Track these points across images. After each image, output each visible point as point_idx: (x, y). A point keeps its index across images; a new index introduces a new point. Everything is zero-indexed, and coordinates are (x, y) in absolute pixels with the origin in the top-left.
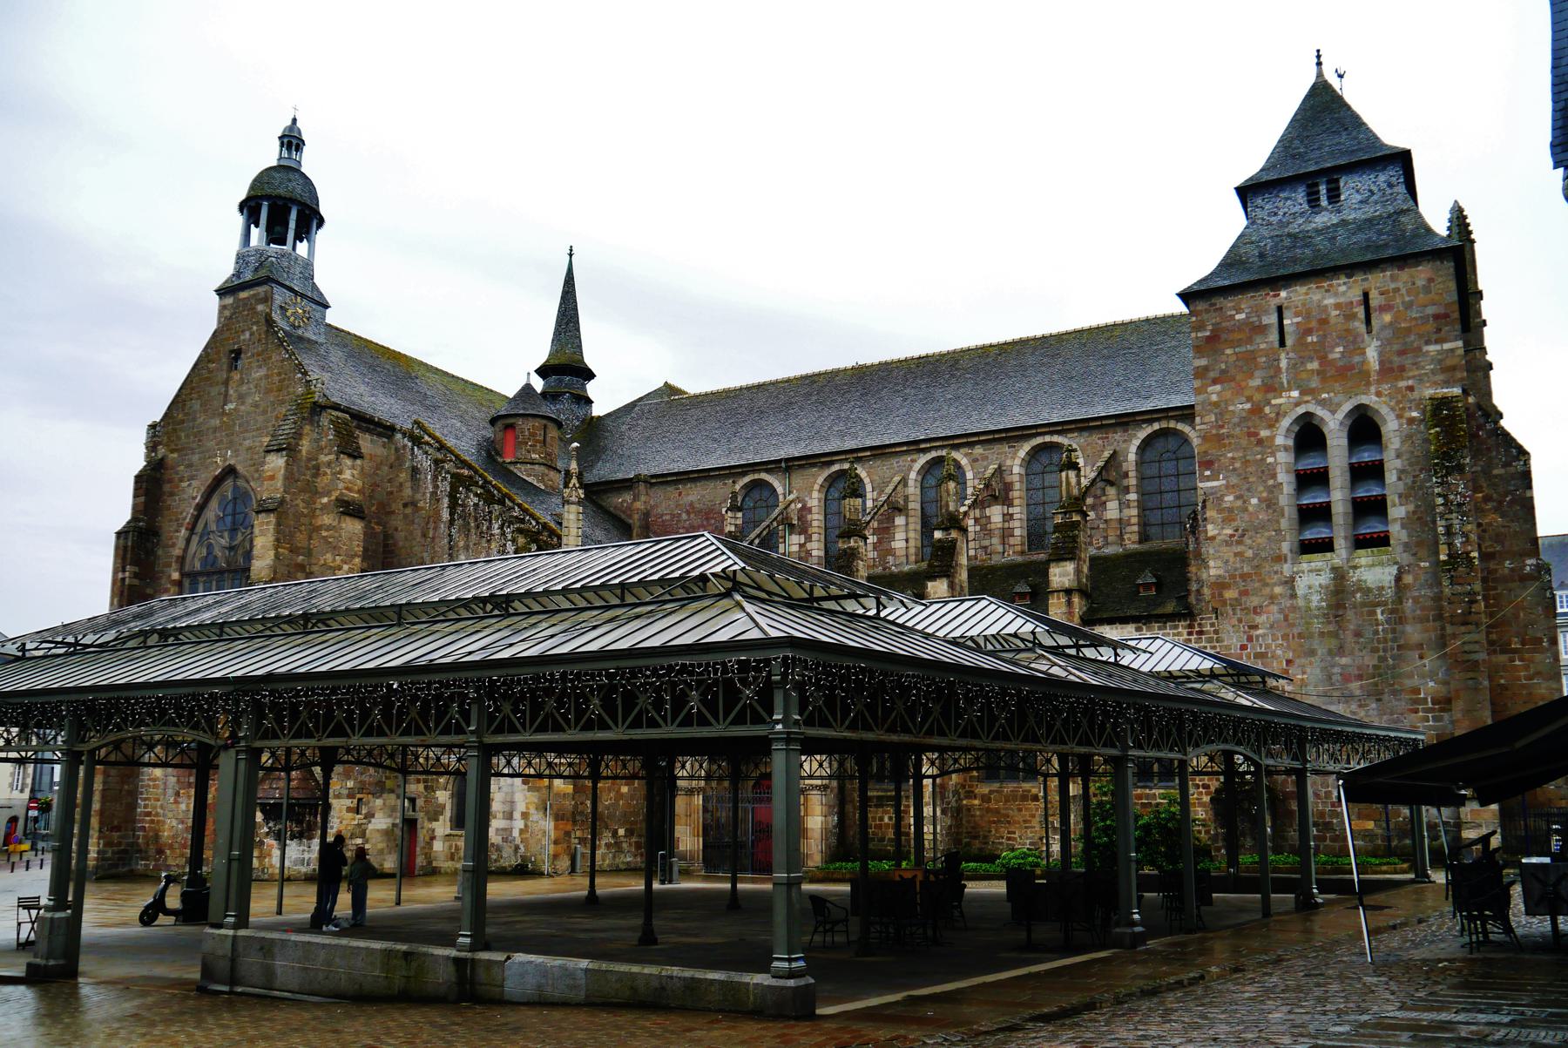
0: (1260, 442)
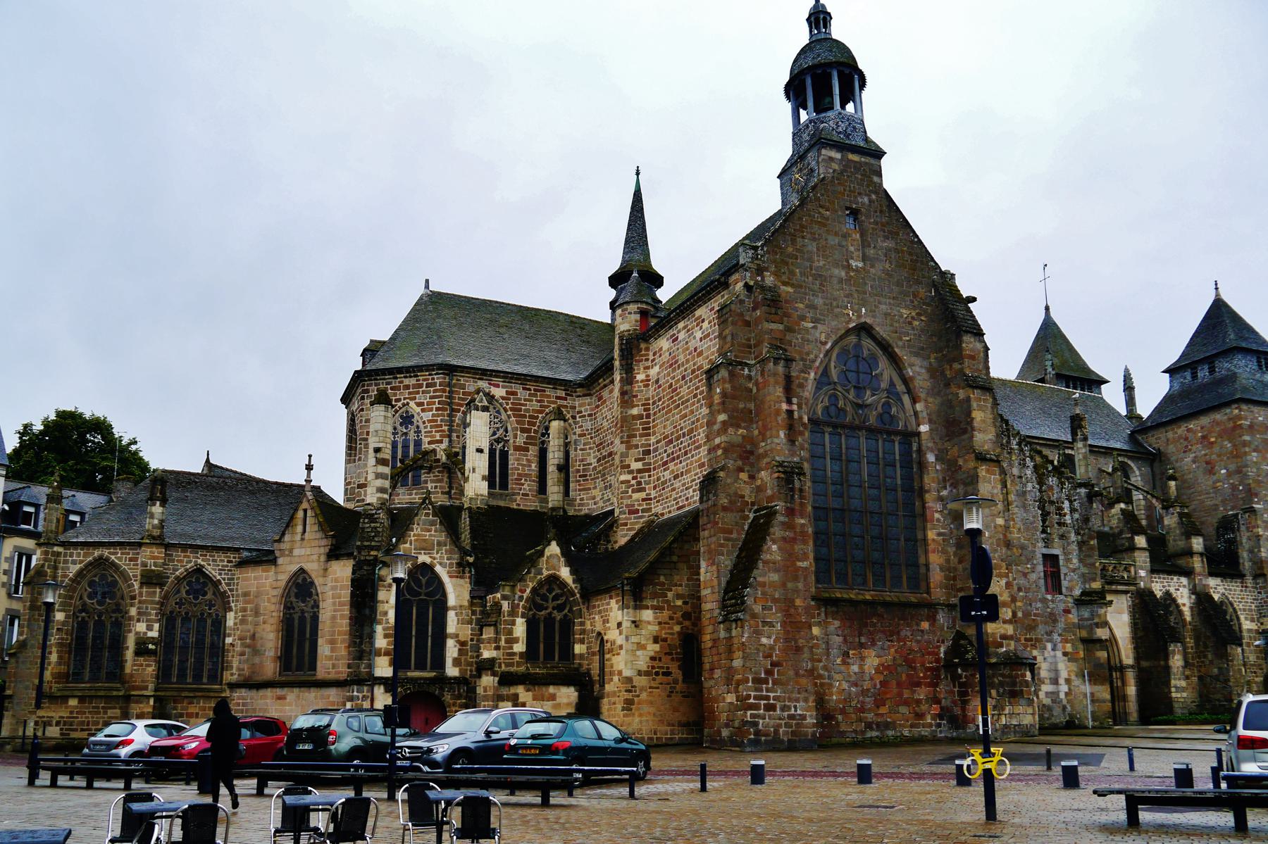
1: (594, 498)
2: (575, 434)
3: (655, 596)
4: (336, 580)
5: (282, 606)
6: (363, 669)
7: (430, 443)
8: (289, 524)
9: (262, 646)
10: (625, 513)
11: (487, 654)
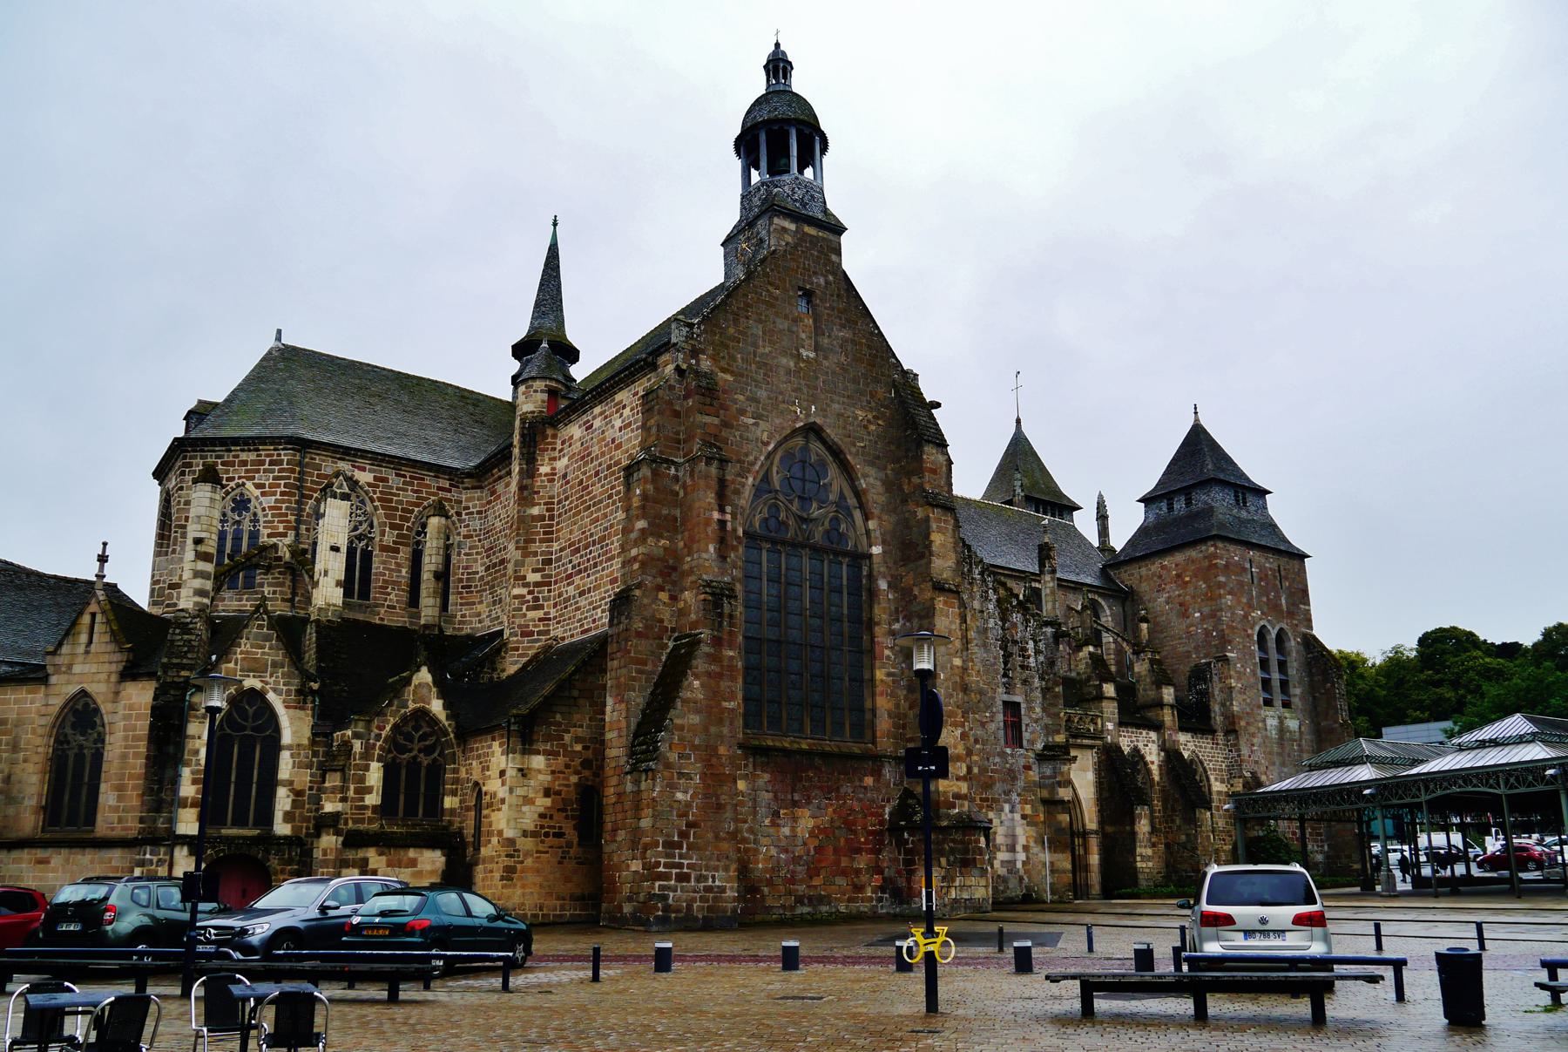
0: (1248, 636)
1: (479, 615)
2: (459, 534)
3: (548, 738)
4: (131, 708)
5: (52, 739)
6: (161, 825)
7: (269, 536)
8: (70, 631)
9: (19, 792)
10: (517, 636)
11: (329, 807)
